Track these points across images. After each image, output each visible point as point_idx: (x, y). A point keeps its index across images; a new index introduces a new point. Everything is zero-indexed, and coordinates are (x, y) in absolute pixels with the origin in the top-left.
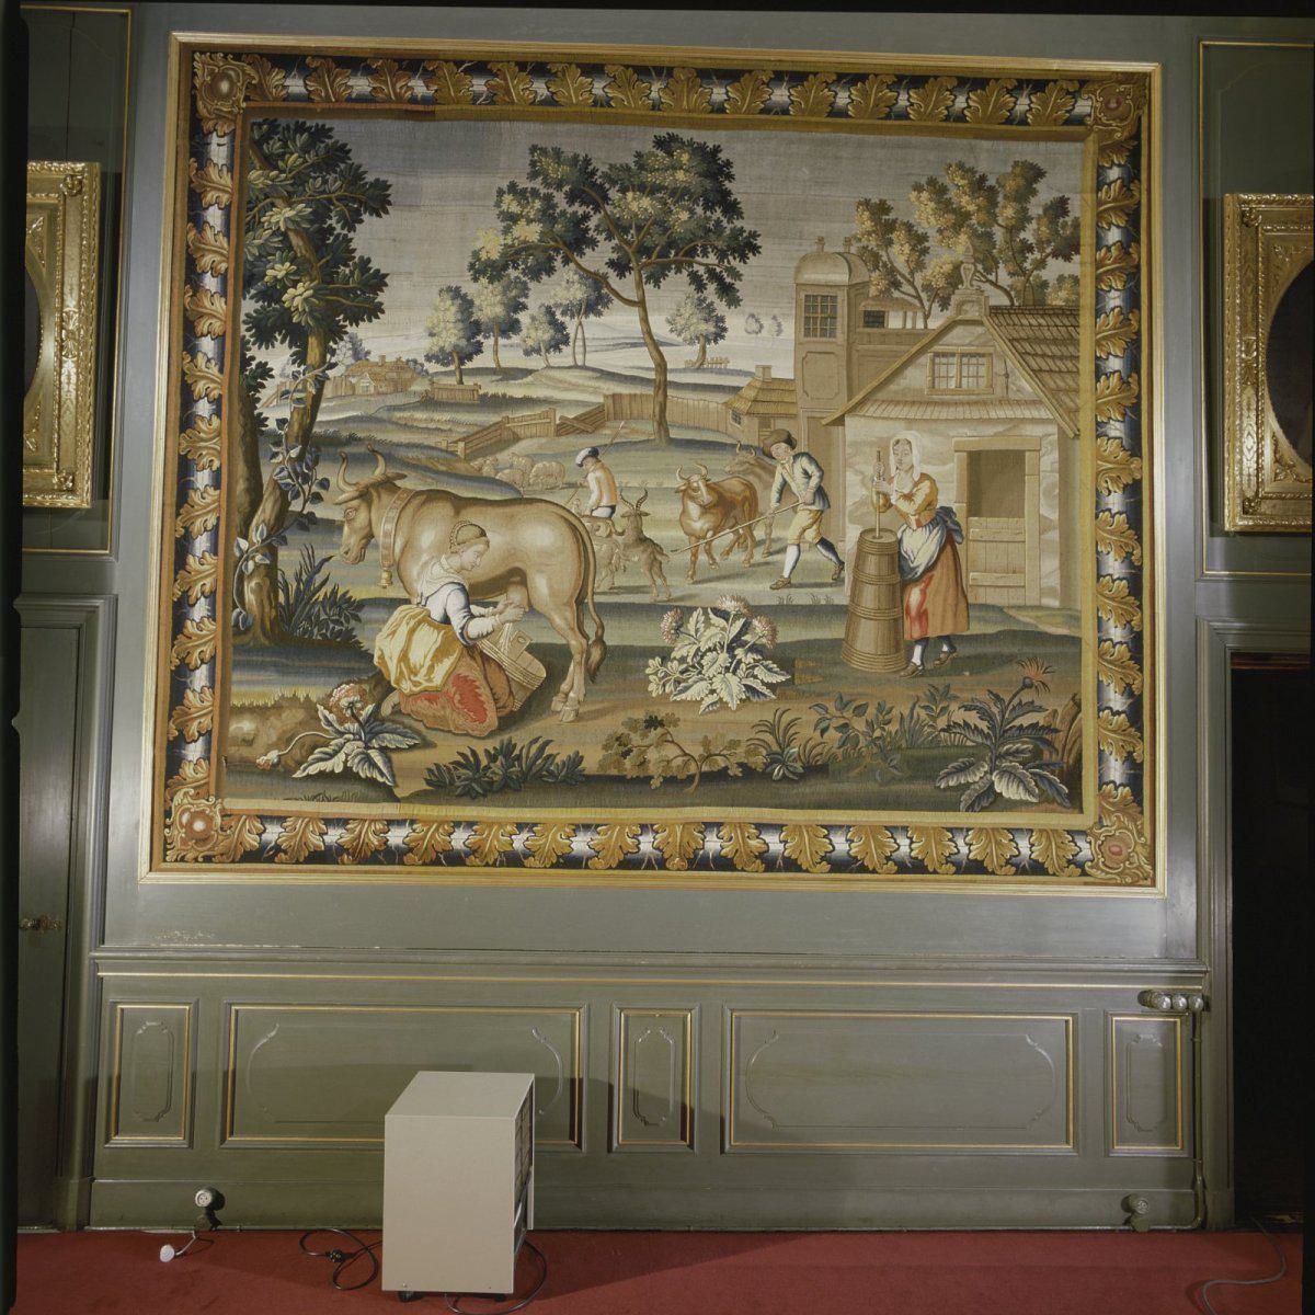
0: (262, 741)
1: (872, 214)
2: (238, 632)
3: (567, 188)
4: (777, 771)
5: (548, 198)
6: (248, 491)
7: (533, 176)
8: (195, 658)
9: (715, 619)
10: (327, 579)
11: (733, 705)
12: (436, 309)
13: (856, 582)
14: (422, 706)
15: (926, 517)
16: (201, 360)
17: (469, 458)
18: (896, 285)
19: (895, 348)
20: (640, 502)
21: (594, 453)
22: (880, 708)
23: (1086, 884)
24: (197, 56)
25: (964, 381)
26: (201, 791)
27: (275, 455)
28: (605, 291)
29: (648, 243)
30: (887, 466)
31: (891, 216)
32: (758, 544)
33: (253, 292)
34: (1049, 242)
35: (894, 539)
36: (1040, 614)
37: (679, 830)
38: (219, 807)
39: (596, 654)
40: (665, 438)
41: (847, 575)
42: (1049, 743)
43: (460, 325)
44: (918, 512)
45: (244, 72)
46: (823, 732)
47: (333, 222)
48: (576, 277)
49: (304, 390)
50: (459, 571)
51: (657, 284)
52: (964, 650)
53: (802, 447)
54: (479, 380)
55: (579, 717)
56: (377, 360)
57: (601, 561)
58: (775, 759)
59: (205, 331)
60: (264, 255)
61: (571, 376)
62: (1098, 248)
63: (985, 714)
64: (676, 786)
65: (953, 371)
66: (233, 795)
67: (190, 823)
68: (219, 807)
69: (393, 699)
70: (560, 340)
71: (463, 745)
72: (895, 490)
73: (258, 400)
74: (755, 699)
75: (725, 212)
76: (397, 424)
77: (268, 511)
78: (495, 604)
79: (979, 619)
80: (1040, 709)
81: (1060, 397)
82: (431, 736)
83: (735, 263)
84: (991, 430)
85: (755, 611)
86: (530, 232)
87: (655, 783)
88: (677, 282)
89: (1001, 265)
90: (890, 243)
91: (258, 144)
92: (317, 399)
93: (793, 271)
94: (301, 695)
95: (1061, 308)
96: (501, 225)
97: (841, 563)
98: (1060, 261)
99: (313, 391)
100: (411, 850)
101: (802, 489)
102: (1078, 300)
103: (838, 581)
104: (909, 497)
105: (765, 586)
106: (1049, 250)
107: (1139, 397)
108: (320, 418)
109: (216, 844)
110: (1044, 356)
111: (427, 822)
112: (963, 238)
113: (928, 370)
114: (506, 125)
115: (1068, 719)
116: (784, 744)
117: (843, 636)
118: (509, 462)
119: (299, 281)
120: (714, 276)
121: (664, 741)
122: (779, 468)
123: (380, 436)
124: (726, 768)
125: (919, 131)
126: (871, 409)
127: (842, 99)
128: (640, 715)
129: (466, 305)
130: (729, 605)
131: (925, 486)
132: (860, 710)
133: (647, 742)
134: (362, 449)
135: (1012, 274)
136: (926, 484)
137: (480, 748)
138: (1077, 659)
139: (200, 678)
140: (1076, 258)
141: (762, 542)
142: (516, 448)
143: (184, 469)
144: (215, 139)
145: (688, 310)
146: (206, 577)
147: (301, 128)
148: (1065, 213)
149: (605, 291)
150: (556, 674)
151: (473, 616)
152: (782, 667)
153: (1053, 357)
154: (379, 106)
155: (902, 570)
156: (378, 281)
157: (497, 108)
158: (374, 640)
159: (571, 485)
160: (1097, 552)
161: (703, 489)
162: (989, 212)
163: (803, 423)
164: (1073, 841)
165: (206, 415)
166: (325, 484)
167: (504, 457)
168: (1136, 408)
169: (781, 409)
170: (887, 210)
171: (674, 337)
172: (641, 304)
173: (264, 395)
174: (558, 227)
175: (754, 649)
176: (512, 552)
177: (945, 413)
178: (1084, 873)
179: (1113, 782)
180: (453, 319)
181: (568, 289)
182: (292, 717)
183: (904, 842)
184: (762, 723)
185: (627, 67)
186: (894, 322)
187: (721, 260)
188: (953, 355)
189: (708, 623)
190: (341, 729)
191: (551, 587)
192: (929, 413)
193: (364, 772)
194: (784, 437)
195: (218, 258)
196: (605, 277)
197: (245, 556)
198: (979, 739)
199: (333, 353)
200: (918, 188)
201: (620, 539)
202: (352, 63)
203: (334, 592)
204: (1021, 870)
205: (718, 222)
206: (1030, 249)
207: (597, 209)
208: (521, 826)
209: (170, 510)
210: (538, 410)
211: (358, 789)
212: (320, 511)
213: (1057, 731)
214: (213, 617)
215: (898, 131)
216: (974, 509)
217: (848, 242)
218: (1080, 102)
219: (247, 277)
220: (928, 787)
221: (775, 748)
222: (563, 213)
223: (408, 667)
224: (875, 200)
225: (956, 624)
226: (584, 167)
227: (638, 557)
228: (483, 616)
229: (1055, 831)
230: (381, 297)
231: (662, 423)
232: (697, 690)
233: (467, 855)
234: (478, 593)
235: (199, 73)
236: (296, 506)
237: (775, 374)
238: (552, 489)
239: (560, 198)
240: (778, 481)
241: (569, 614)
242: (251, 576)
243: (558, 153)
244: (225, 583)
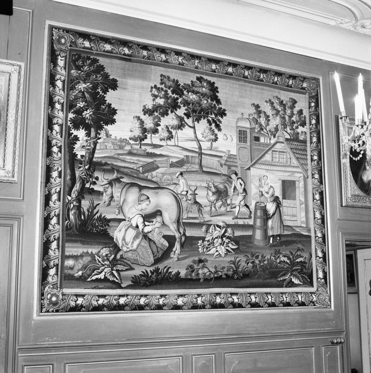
0: (76, 268)
1: (255, 108)
2: (67, 229)
3: (172, 89)
4: (236, 277)
5: (166, 91)
6: (71, 179)
7: (162, 84)
8: (52, 238)
9: (217, 228)
11: (223, 255)
12: (133, 123)
13: (255, 217)
14: (130, 255)
15: (272, 199)
16: (54, 133)
17: (143, 173)
18: (262, 129)
19: (262, 148)
20: (195, 190)
21: (181, 174)
22: (262, 256)
23: (315, 308)
24: (54, 29)
25: (280, 159)
26: (54, 286)
27: (80, 167)
29: (195, 109)
30: (262, 183)
31: (260, 109)
32: (228, 205)
33: (72, 111)
34: (299, 121)
35: (264, 205)
36: (301, 228)
37: (209, 296)
39: (183, 239)
41: (252, 215)
42: (305, 267)
43: (140, 129)
44: (270, 198)
45: (70, 37)
46: (248, 263)
47: (99, 90)
48: (175, 117)
49: (90, 146)
51: (198, 122)
52: (283, 239)
53: (239, 176)
55: (179, 259)
56: (114, 138)
57: (184, 209)
58: (235, 272)
59: (56, 123)
60: (76, 98)
62: (310, 125)
63: (289, 258)
64: (208, 282)
65: (277, 156)
66: (66, 288)
67: (51, 298)
68: (61, 292)
71: (143, 269)
73: (74, 148)
74: (229, 254)
75: (216, 102)
76: (121, 160)
79: (286, 230)
80: (302, 257)
81: (303, 165)
82: (133, 266)
83: (220, 118)
85: (228, 226)
86: (161, 101)
87: (202, 281)
88: (204, 122)
89: (288, 127)
90: (260, 117)
91: (74, 62)
92: (94, 149)
95: (302, 140)
96: (152, 98)
97: (251, 212)
98: (302, 127)
99: (93, 146)
101: (240, 189)
102: (306, 139)
104: (267, 193)
106: (299, 124)
107: (321, 167)
108: (95, 155)
109: (60, 306)
110: (299, 154)
111: (132, 295)
112: (278, 118)
113: (270, 155)
114: (153, 67)
115: (309, 259)
116: (237, 268)
117: (252, 234)
119: (88, 109)
120: (214, 122)
121: (203, 267)
122: (233, 182)
123: (115, 164)
124: (221, 276)
126: (257, 166)
128: (197, 259)
129: (142, 123)
130: (221, 224)
132: (257, 257)
133: (199, 267)
134: (109, 167)
135: (290, 130)
136: (272, 189)
137: (149, 270)
138: (310, 242)
139: (54, 245)
140: (305, 127)
141: (228, 205)
142: (158, 170)
143: (48, 170)
144: (59, 58)
145: (207, 131)
147: (89, 58)
148: (302, 114)
149: (183, 122)
150: (171, 245)
151: (145, 226)
152: (236, 243)
153: (301, 154)
154: (114, 55)
155: (266, 214)
156: (114, 112)
157: (149, 61)
158: (114, 233)
160: (314, 211)
161: (213, 187)
162: (284, 111)
163: (239, 168)
164: (311, 296)
165: (56, 152)
166: (97, 178)
167: (154, 173)
168: (321, 170)
169: (234, 164)
171: (203, 139)
173: (76, 146)
174: (169, 101)
175: (228, 238)
176: (157, 206)
178: (314, 305)
179: (320, 278)
183: (270, 297)
184: (231, 261)
185: (188, 54)
186: (262, 140)
187: (216, 117)
188: (277, 151)
189: (215, 229)
190: (103, 263)
193: (111, 278)
194: (234, 172)
195: (60, 98)
196: (183, 118)
197: (70, 202)
198: (288, 266)
199: (99, 134)
200: (266, 102)
201: (190, 202)
202: (107, 40)
203: (101, 216)
205: (215, 105)
206: (294, 123)
207: (180, 97)
209: (43, 184)
210: (164, 159)
211: (109, 284)
212: (96, 188)
213: (306, 263)
214: (58, 223)
215: (261, 85)
216: (284, 198)
217: (249, 115)
218: (304, 84)
219: (71, 106)
220: (275, 280)
221: (235, 269)
222: (171, 96)
224: (256, 104)
225: (281, 231)
226: (176, 82)
227: (195, 208)
228: (148, 225)
229: (307, 293)
230: (115, 117)
232: (213, 251)
233: (145, 306)
235: (55, 35)
236: (87, 185)
237: (232, 153)
238: (169, 185)
239: (169, 92)
242: (72, 209)
243: (169, 77)
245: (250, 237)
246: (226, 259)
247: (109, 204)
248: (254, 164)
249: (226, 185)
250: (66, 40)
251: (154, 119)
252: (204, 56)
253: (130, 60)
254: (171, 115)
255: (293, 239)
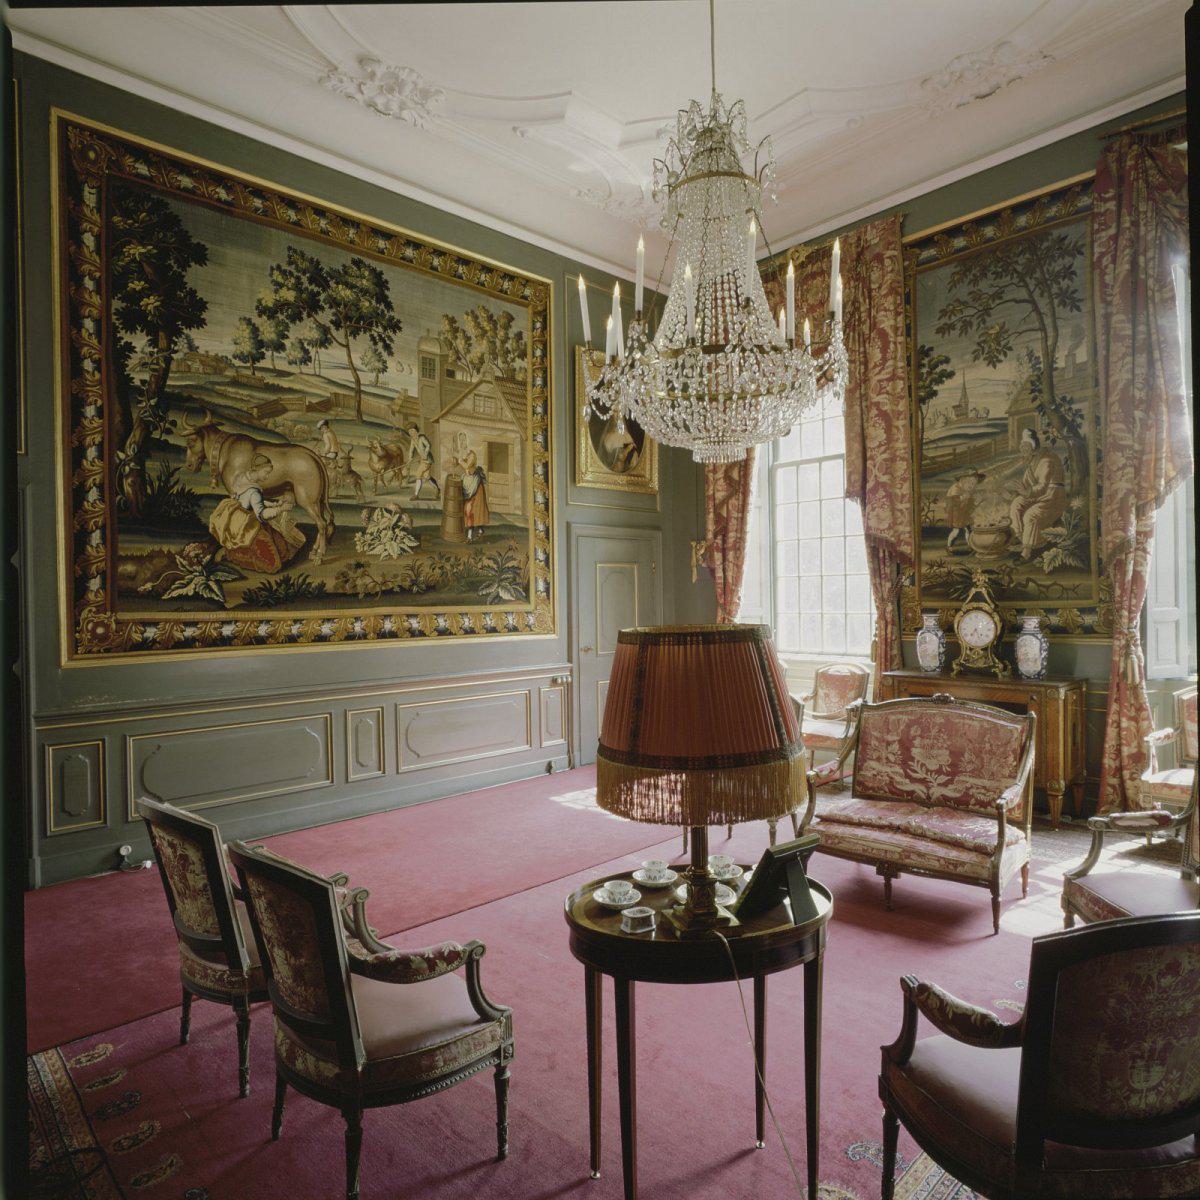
3: (308, 275)
4: (415, 589)
7: (290, 263)
9: (386, 514)
10: (177, 482)
11: (395, 556)
13: (445, 499)
17: (261, 417)
21: (326, 423)
24: (70, 128)
26: (101, 609)
27: (140, 402)
28: (329, 336)
29: (349, 314)
31: (457, 325)
32: (404, 477)
33: (119, 295)
37: (372, 619)
38: (114, 618)
39: (330, 530)
40: (360, 420)
41: (442, 496)
42: (518, 574)
43: (252, 341)
45: (105, 149)
49: (158, 364)
50: (257, 481)
51: (355, 337)
52: (488, 533)
54: (264, 374)
56: (203, 352)
58: (414, 583)
59: (87, 314)
60: (127, 271)
61: (313, 380)
64: (371, 598)
65: (482, 402)
66: (123, 611)
67: (94, 630)
68: (114, 618)
69: (222, 552)
70: (306, 359)
71: (263, 578)
72: (461, 456)
73: (127, 366)
76: (216, 392)
77: (137, 437)
78: (277, 501)
79: (494, 519)
80: (515, 559)
81: (521, 421)
82: (245, 573)
83: (391, 334)
84: (495, 433)
85: (403, 511)
86: (289, 295)
87: (361, 596)
90: (456, 338)
92: (167, 371)
93: (416, 344)
94: (165, 549)
98: (520, 360)
100: (235, 637)
101: (423, 453)
103: (438, 498)
104: (465, 461)
105: (408, 499)
108: (169, 382)
109: (113, 640)
111: (245, 621)
114: (274, 231)
116: (418, 576)
118: (282, 422)
119: (151, 295)
121: (364, 574)
123: (207, 399)
125: (467, 286)
127: (436, 262)
128: (353, 562)
129: (255, 330)
130: (392, 507)
131: (472, 457)
134: (197, 405)
137: (273, 579)
138: (528, 536)
139: (96, 537)
141: (404, 477)
142: (285, 416)
145: (370, 354)
146: (97, 474)
150: (311, 540)
154: (196, 198)
156: (202, 306)
157: (267, 218)
158: (208, 518)
159: (315, 439)
163: (422, 420)
165: (90, 369)
166: (174, 423)
167: (279, 419)
168: (546, 430)
169: (413, 412)
170: (455, 322)
172: (347, 346)
174: (304, 296)
175: (404, 529)
176: (285, 474)
177: (478, 423)
180: (247, 336)
181: (310, 331)
182: (159, 562)
183: (466, 620)
186: (459, 376)
188: (481, 396)
190: (191, 569)
191: (307, 493)
192: (472, 422)
193: (206, 594)
196: (329, 328)
197: (124, 463)
199: (176, 343)
200: (467, 314)
203: (183, 489)
204: (510, 630)
205: (383, 311)
207: (324, 290)
208: (296, 621)
210: (296, 396)
211: (203, 604)
212: (172, 440)
213: (520, 569)
215: (458, 284)
216: (491, 469)
221: (414, 578)
223: (230, 534)
227: (349, 480)
228: (270, 507)
230: (204, 315)
231: (359, 411)
232: (378, 550)
233: (267, 638)
234: (268, 494)
235: (73, 140)
236: (156, 435)
238: (305, 440)
239: (304, 279)
240: (412, 447)
241: (316, 508)
242: (127, 476)
243: (302, 255)
244: (111, 480)
245: (437, 529)
246: (400, 562)
247: (198, 470)
248: (446, 414)
249: (401, 445)
250: (98, 156)
251: (277, 325)
252: (365, 223)
253: (230, 213)
254: (308, 322)
255: (503, 533)
